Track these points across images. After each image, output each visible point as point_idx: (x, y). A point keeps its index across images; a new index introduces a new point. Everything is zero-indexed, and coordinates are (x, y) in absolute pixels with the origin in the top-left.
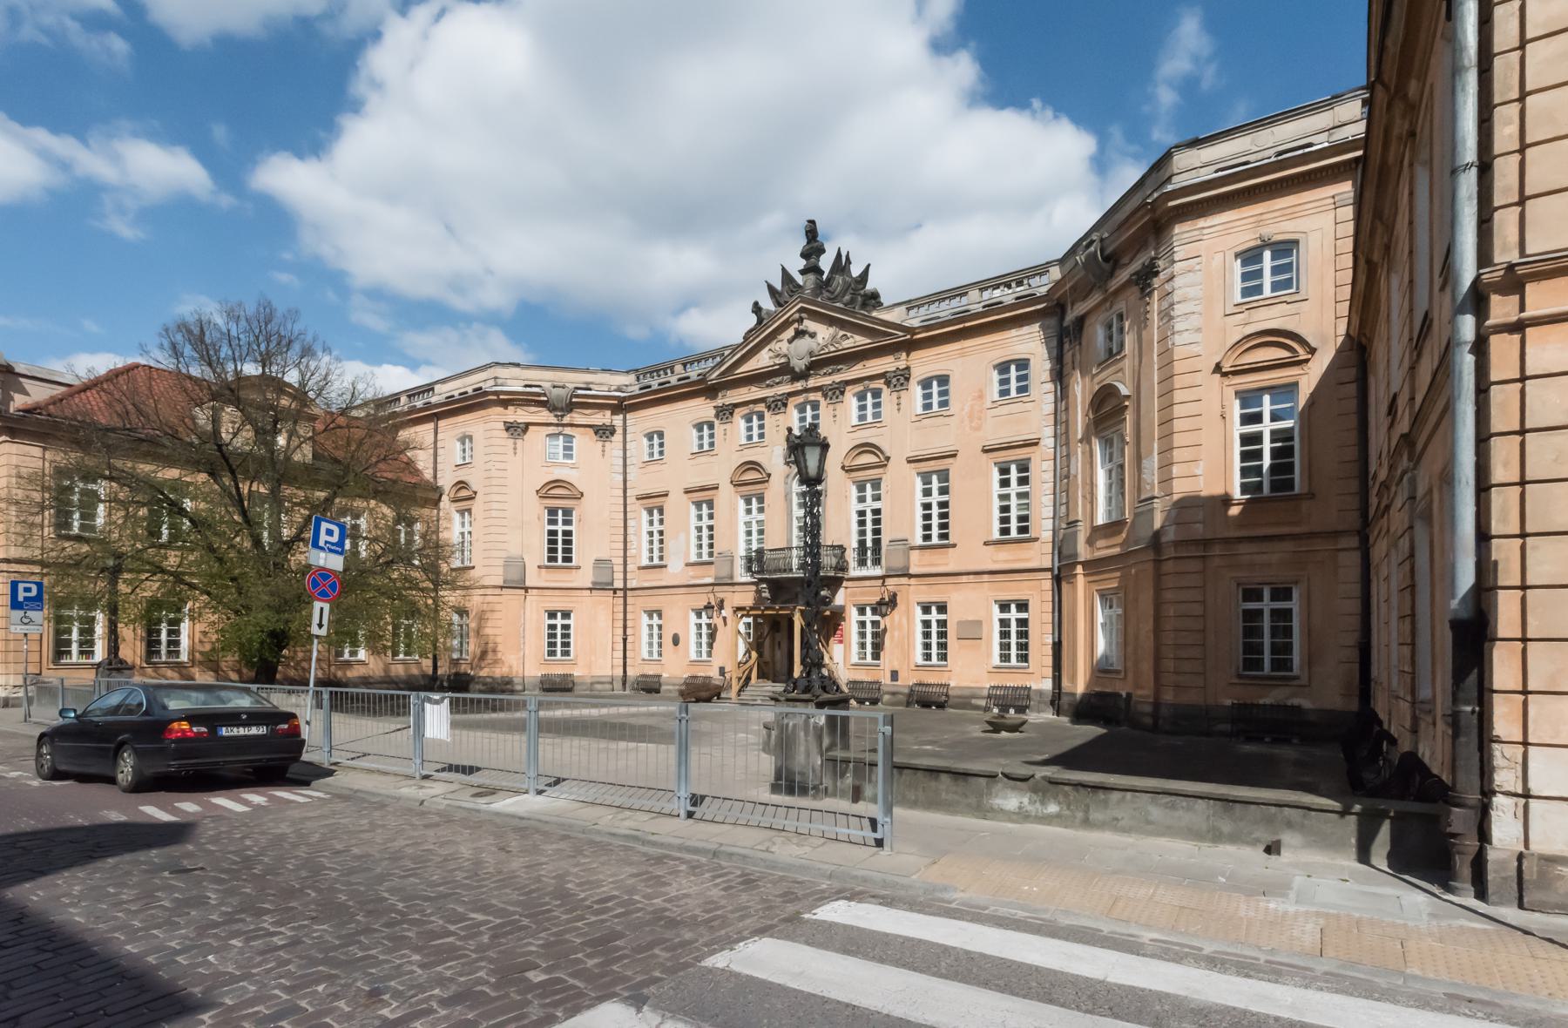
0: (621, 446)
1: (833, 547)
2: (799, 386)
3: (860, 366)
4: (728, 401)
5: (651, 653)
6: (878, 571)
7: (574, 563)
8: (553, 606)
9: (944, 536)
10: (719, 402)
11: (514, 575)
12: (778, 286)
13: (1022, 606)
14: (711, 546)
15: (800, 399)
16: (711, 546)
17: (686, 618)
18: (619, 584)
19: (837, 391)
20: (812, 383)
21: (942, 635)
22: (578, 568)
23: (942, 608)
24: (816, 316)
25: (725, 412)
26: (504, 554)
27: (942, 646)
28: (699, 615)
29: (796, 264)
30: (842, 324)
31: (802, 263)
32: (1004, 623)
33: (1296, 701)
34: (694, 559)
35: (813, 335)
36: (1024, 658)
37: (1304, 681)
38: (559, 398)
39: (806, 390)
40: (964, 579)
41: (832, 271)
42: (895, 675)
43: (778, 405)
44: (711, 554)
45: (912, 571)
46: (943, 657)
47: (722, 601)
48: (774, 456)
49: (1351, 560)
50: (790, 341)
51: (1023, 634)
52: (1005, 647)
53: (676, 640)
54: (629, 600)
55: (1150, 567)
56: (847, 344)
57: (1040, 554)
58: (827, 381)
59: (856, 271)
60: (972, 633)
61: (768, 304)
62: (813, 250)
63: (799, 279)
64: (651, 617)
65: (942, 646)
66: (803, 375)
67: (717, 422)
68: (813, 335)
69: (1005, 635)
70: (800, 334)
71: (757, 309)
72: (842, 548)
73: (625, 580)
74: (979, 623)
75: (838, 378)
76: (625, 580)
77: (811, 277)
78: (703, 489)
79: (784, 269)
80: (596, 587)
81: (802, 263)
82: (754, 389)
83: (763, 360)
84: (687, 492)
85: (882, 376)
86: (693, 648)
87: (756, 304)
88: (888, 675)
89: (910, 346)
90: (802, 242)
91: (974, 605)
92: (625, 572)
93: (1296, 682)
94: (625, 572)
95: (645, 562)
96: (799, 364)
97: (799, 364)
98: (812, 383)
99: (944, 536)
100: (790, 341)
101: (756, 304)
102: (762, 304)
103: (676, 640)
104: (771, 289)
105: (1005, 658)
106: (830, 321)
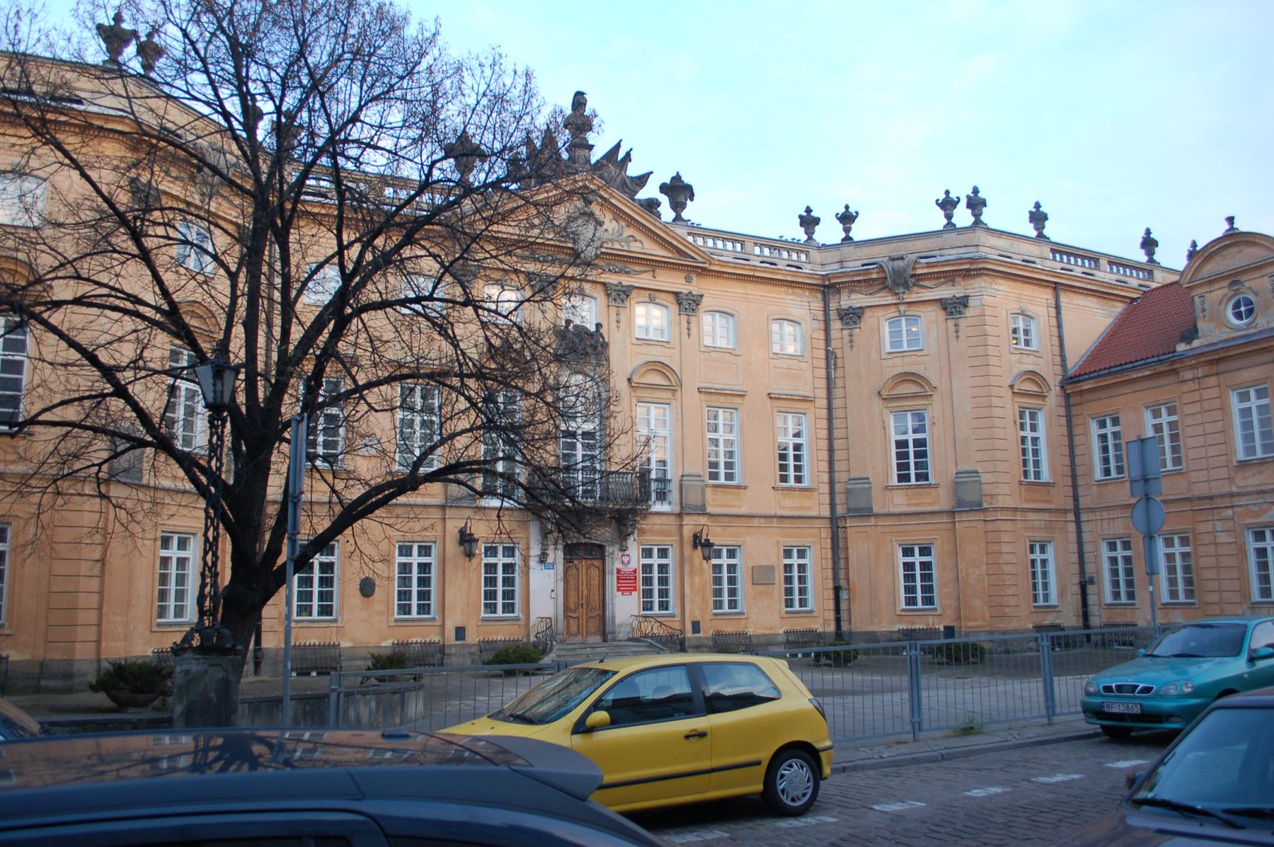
3: (648, 276)
5: (1116, 595)
8: (908, 539)
19: (619, 295)
21: (732, 581)
30: (632, 222)
32: (788, 568)
40: (756, 522)
45: (709, 510)
49: (1072, 527)
51: (927, 577)
53: (367, 588)
56: (635, 247)
58: (613, 279)
59: (633, 170)
60: (761, 576)
74: (773, 567)
75: (626, 281)
85: (676, 294)
88: (689, 627)
89: (704, 272)
91: (760, 549)
105: (789, 603)
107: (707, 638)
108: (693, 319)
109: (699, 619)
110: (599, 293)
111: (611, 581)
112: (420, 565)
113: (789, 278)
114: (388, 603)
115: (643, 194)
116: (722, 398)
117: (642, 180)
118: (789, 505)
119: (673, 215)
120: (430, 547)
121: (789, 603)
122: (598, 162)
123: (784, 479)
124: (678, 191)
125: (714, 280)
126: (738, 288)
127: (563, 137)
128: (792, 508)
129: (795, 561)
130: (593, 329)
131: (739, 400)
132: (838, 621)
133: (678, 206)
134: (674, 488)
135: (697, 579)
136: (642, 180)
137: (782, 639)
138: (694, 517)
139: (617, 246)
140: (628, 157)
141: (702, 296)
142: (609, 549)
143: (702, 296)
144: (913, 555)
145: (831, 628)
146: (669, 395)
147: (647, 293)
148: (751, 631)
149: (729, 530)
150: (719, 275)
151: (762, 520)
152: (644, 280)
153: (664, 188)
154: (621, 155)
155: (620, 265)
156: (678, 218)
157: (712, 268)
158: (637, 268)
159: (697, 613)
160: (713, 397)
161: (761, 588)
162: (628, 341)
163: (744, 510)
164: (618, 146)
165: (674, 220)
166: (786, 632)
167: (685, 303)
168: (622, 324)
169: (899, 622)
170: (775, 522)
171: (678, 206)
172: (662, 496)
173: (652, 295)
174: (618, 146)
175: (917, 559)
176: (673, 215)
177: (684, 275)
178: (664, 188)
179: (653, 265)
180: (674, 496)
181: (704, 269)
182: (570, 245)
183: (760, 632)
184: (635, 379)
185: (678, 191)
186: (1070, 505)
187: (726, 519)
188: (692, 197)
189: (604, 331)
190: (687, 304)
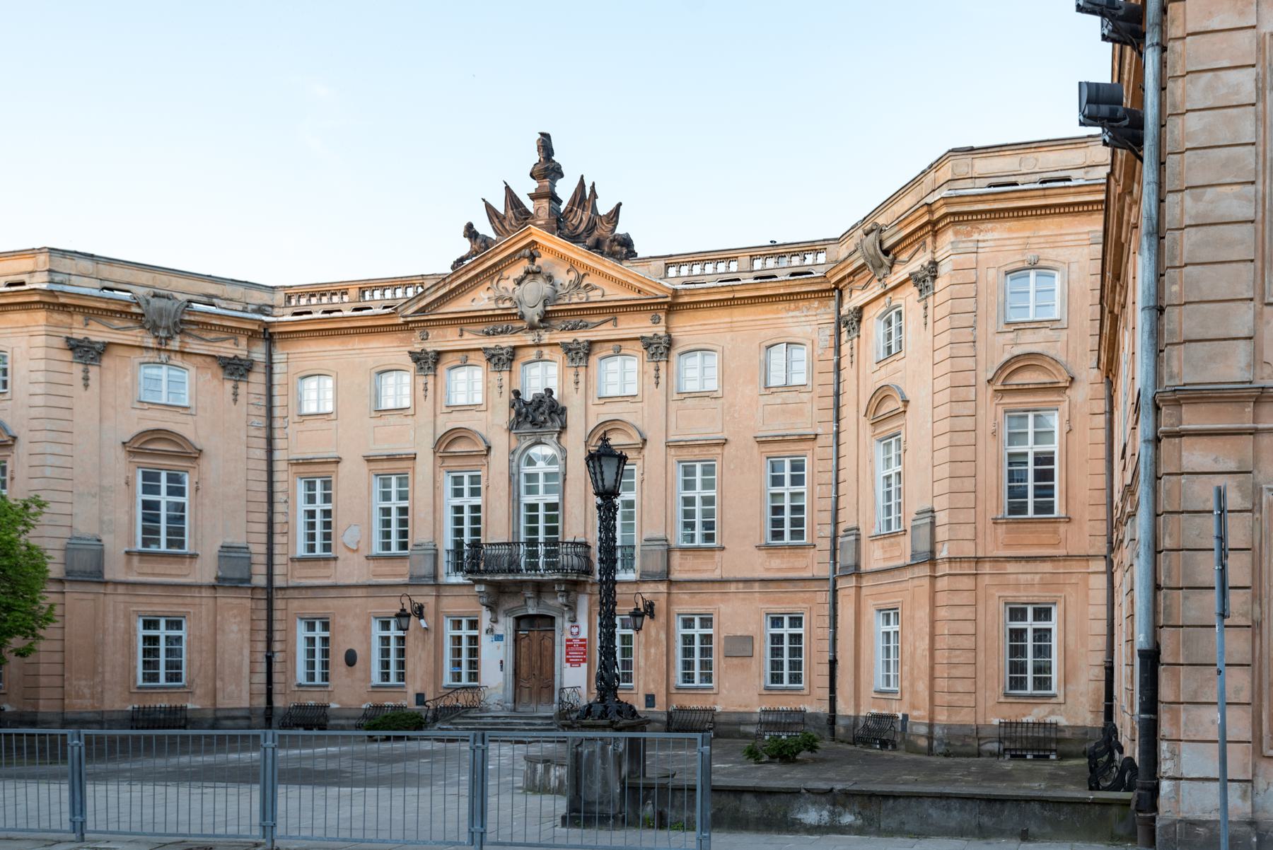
0: (262, 389)
1: (575, 544)
2: (529, 338)
3: (608, 326)
4: (431, 346)
6: (631, 576)
7: (187, 549)
9: (709, 538)
10: (417, 348)
11: (83, 562)
12: (500, 207)
13: (796, 621)
14: (404, 534)
15: (533, 353)
16: (404, 534)
17: (367, 630)
18: (260, 580)
19: (581, 354)
21: (706, 652)
22: (193, 556)
23: (706, 622)
25: (427, 362)
26: (66, 532)
27: (706, 665)
28: (385, 625)
29: (525, 188)
31: (533, 185)
32: (777, 639)
33: (1053, 719)
34: (377, 549)
36: (796, 678)
37: (1061, 699)
38: (160, 312)
40: (733, 587)
41: (572, 202)
42: (650, 700)
44: (404, 546)
45: (675, 576)
46: (707, 678)
47: (421, 608)
48: (494, 424)
50: (519, 282)
52: (777, 665)
53: (351, 658)
54: (278, 604)
55: (926, 582)
56: (595, 296)
57: (816, 564)
58: (567, 337)
59: (604, 208)
60: (741, 647)
61: (485, 228)
62: (548, 170)
63: (530, 205)
64: (311, 626)
65: (706, 665)
69: (776, 652)
71: (470, 232)
72: (586, 545)
73: (270, 576)
75: (582, 336)
76: (270, 576)
77: (545, 203)
78: (391, 458)
79: (507, 188)
80: (221, 584)
81: (533, 185)
83: (481, 300)
84: (369, 460)
86: (376, 670)
87: (470, 227)
88: (642, 700)
90: (535, 157)
92: (270, 565)
93: (1053, 700)
94: (270, 565)
95: (301, 551)
96: (533, 314)
98: (546, 337)
99: (709, 538)
100: (519, 282)
101: (470, 227)
102: (477, 228)
103: (351, 658)
105: (777, 678)
107: (661, 713)
109: (653, 692)
110: (559, 355)
111: (560, 652)
112: (791, 636)
113: (782, 291)
114: (368, 671)
116: (696, 451)
118: (776, 566)
120: (180, 622)
121: (777, 678)
123: (778, 535)
125: (692, 313)
126: (721, 318)
128: (779, 570)
129: (786, 630)
131: (718, 450)
132: (833, 701)
134: (637, 552)
135: (653, 651)
137: (756, 718)
138: (652, 585)
140: (594, 195)
142: (558, 621)
144: (1024, 618)
145: (824, 708)
147: (611, 344)
148: (719, 709)
149: (698, 596)
150: (695, 306)
151: (741, 585)
152: (604, 332)
155: (573, 320)
157: (681, 300)
158: (596, 320)
159: (652, 686)
160: (685, 451)
161: (735, 661)
163: (716, 575)
164: (582, 184)
166: (765, 712)
168: (581, 385)
169: (873, 706)
170: (757, 587)
172: (628, 565)
173: (618, 346)
174: (582, 184)
175: (697, 631)
177: (650, 315)
179: (613, 311)
180: (637, 563)
183: (731, 709)
186: (1101, 547)
187: (695, 586)
190: (660, 348)
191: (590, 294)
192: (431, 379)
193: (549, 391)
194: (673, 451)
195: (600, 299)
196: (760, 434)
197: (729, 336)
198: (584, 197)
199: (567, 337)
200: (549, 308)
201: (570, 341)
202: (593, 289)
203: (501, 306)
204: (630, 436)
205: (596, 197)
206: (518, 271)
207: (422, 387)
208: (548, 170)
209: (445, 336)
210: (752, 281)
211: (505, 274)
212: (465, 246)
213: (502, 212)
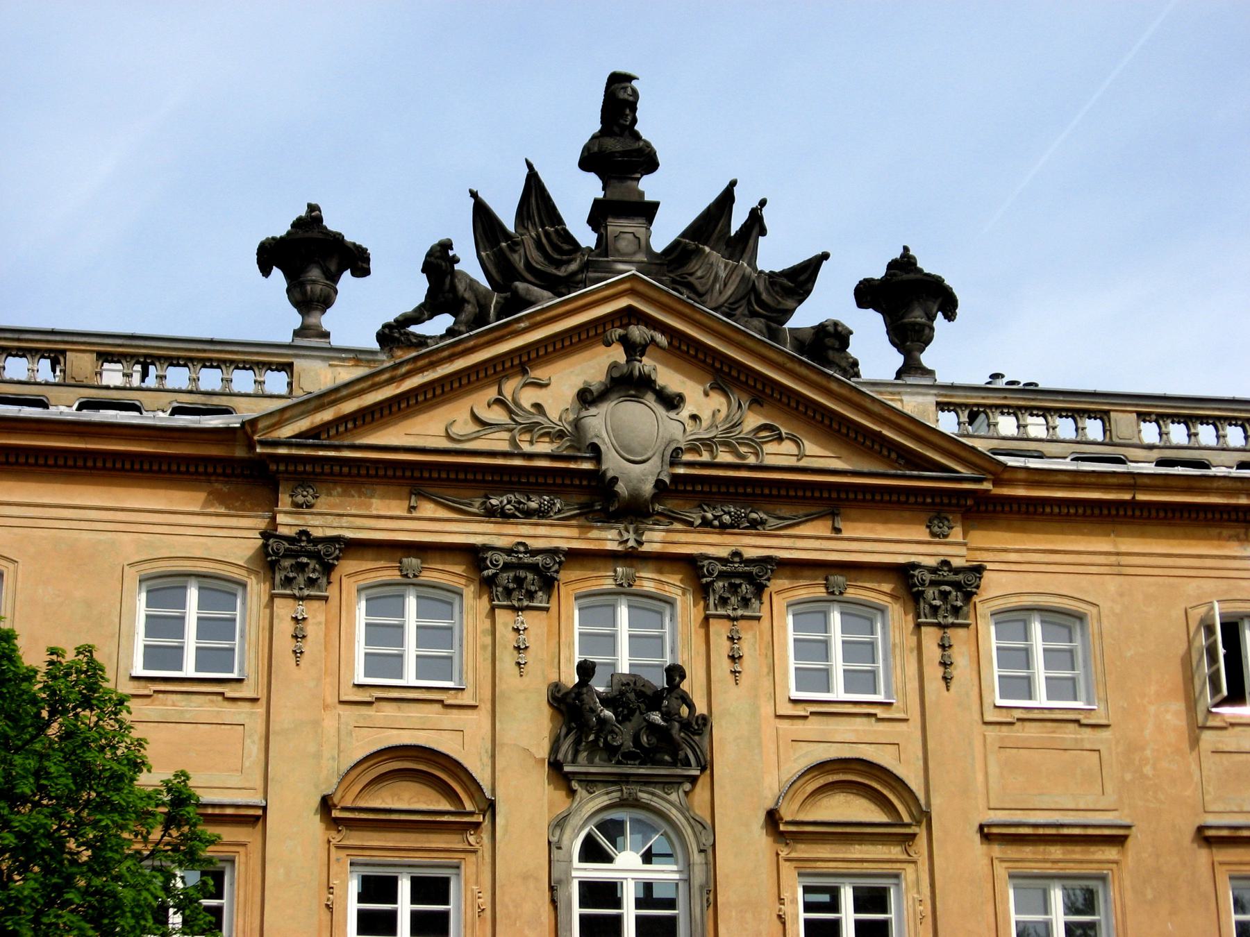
2: (608, 538)
3: (820, 528)
4: (321, 527)
10: (288, 524)
12: (507, 216)
20: (655, 539)
24: (686, 352)
25: (298, 565)
35: (672, 402)
39: (632, 557)
43: (519, 582)
56: (779, 454)
58: (715, 545)
59: (774, 255)
61: (469, 264)
62: (619, 152)
66: (634, 511)
67: (257, 589)
68: (672, 402)
70: (628, 384)
71: (439, 263)
75: (753, 546)
82: (428, 509)
97: (637, 477)
98: (655, 539)
100: (587, 398)
104: (482, 214)
106: (723, 376)
108: (958, 637)
115: (805, 317)
116: (1056, 852)
117: (801, 279)
119: (898, 360)
122: (675, 245)
124: (910, 298)
127: (575, 196)
130: (660, 681)
131: (1111, 853)
133: (909, 338)
136: (801, 279)
139: (725, 457)
140: (756, 223)
141: (978, 570)
143: (978, 570)
146: (895, 852)
152: (809, 540)
153: (867, 294)
154: (738, 219)
156: (911, 367)
160: (1027, 851)
162: (767, 710)
164: (726, 199)
165: (899, 374)
167: (930, 592)
168: (747, 665)
171: (909, 338)
174: (726, 199)
176: (898, 360)
178: (867, 294)
181: (983, 498)
182: (587, 466)
184: (787, 813)
185: (910, 298)
188: (950, 315)
189: (693, 686)
190: (940, 598)
191: (769, 448)
192: (314, 613)
193: (675, 673)
194: (997, 850)
195: (792, 462)
196: (1211, 820)
197: (1112, 584)
198: (723, 229)
199: (715, 545)
200: (681, 471)
201: (724, 553)
202: (780, 439)
203: (526, 448)
204: (883, 803)
205: (763, 232)
206: (594, 365)
207: (284, 628)
208: (619, 152)
209: (369, 506)
210: (1150, 468)
211: (539, 373)
212: (417, 290)
213: (509, 223)
